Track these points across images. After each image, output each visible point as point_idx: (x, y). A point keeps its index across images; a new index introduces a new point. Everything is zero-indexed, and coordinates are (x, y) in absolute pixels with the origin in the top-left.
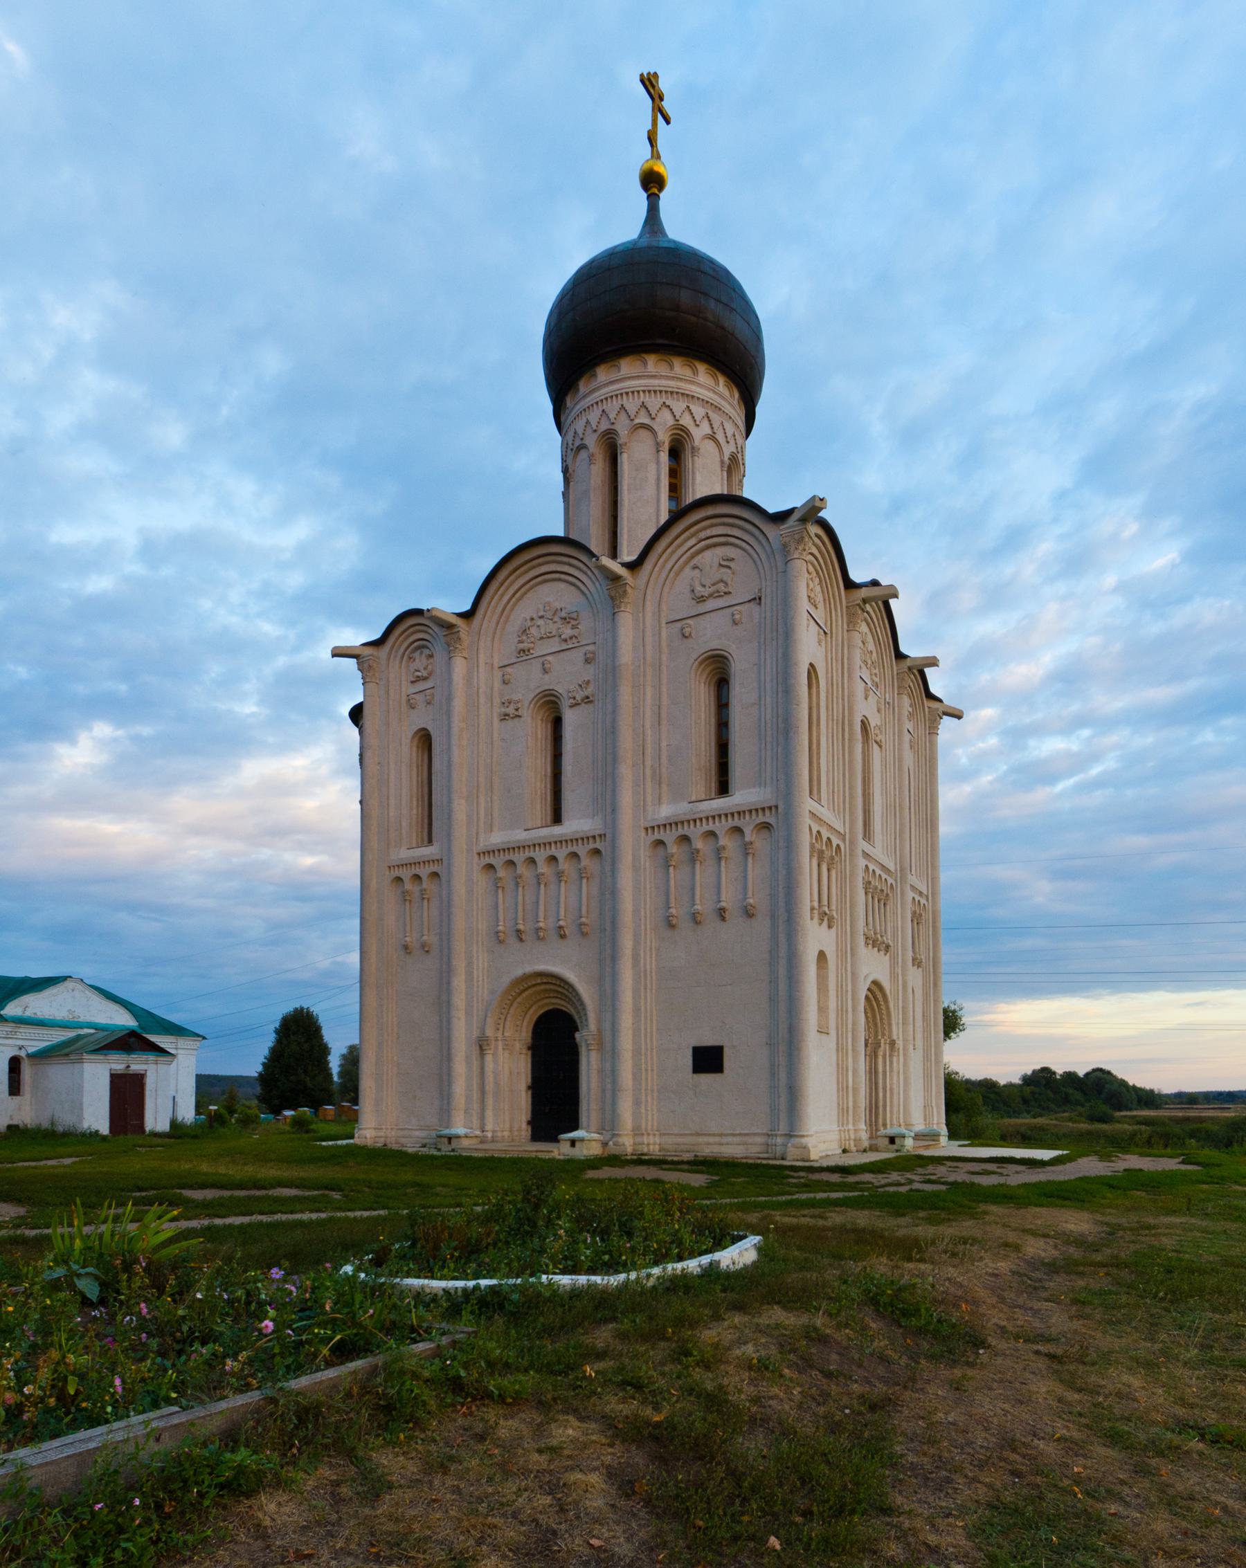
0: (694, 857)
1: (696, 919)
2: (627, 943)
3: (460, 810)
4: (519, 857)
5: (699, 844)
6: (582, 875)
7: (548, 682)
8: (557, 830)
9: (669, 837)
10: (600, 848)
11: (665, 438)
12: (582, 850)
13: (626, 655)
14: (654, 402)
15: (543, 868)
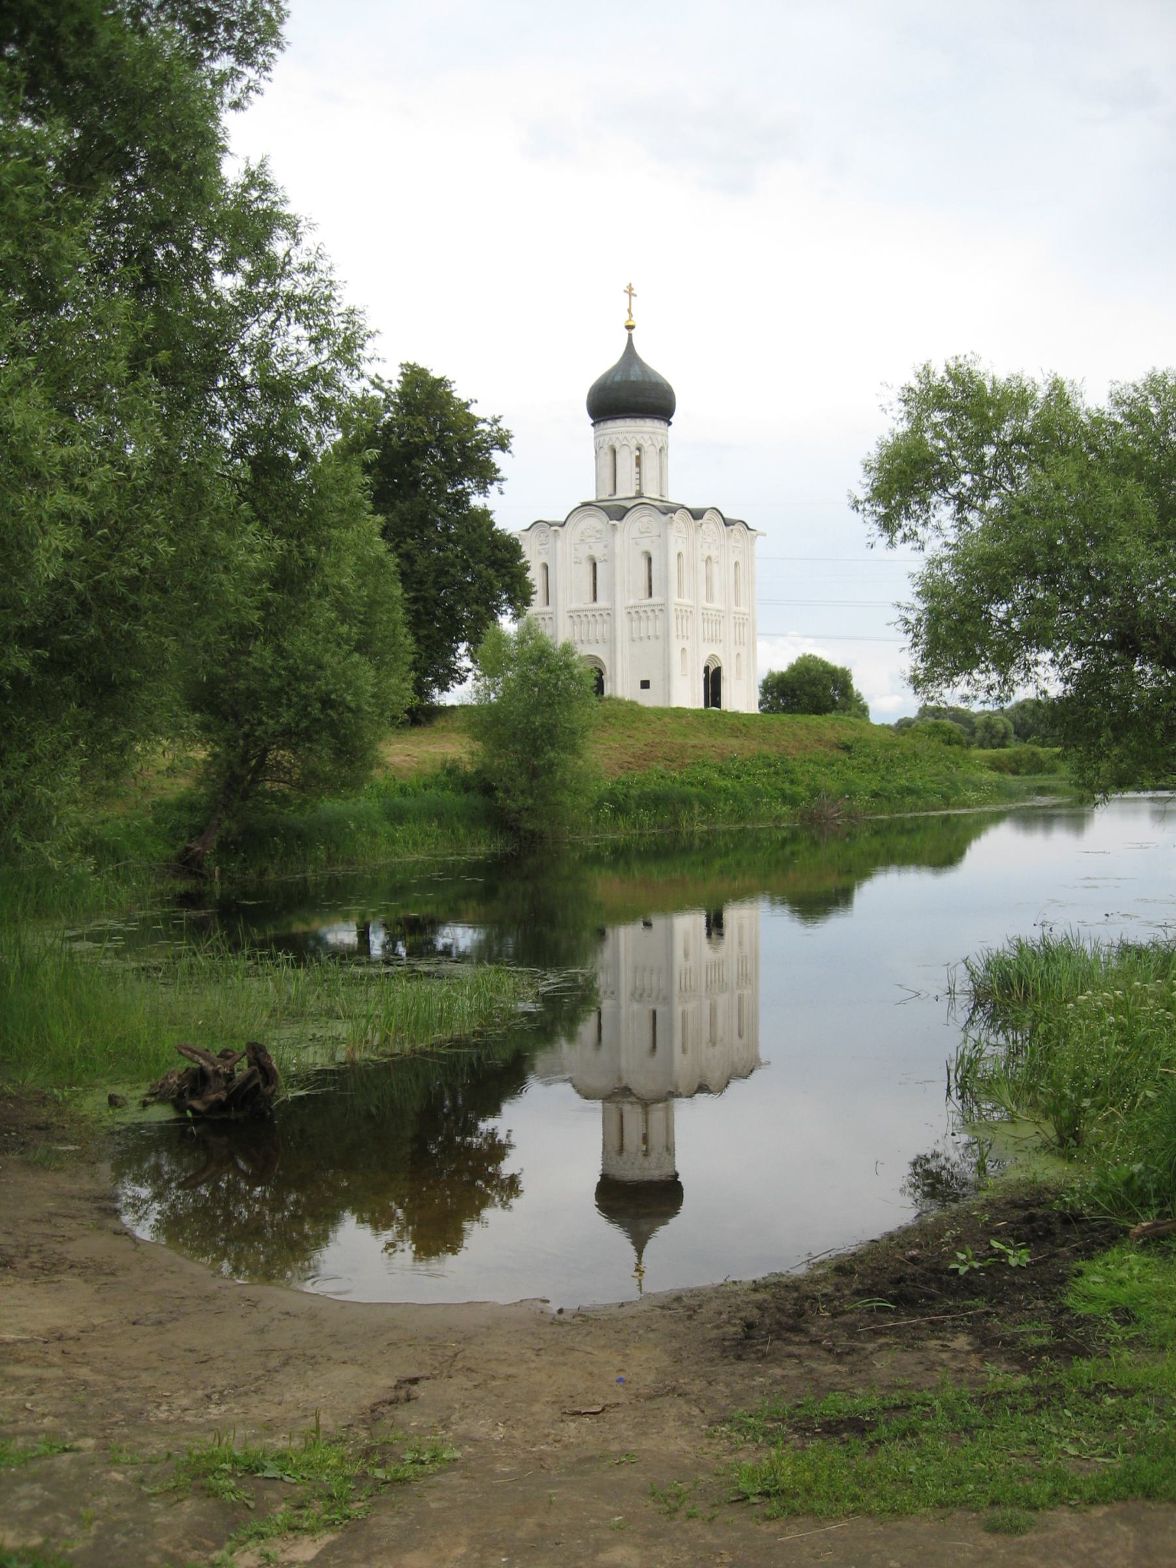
0: (640, 618)
1: (641, 639)
2: (619, 645)
3: (560, 596)
4: (582, 614)
5: (642, 614)
6: (604, 622)
7: (592, 552)
8: (595, 605)
9: (633, 611)
10: (610, 613)
11: (633, 448)
12: (604, 613)
13: (618, 549)
14: (629, 436)
15: (591, 618)
